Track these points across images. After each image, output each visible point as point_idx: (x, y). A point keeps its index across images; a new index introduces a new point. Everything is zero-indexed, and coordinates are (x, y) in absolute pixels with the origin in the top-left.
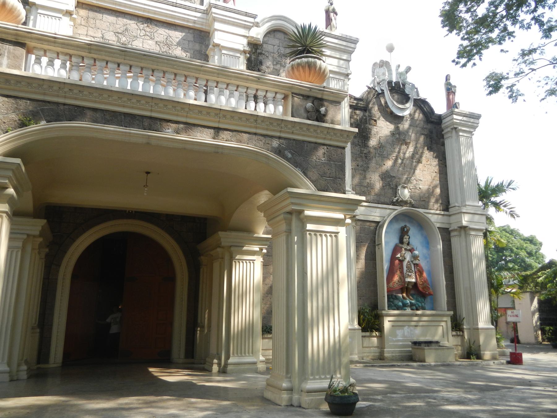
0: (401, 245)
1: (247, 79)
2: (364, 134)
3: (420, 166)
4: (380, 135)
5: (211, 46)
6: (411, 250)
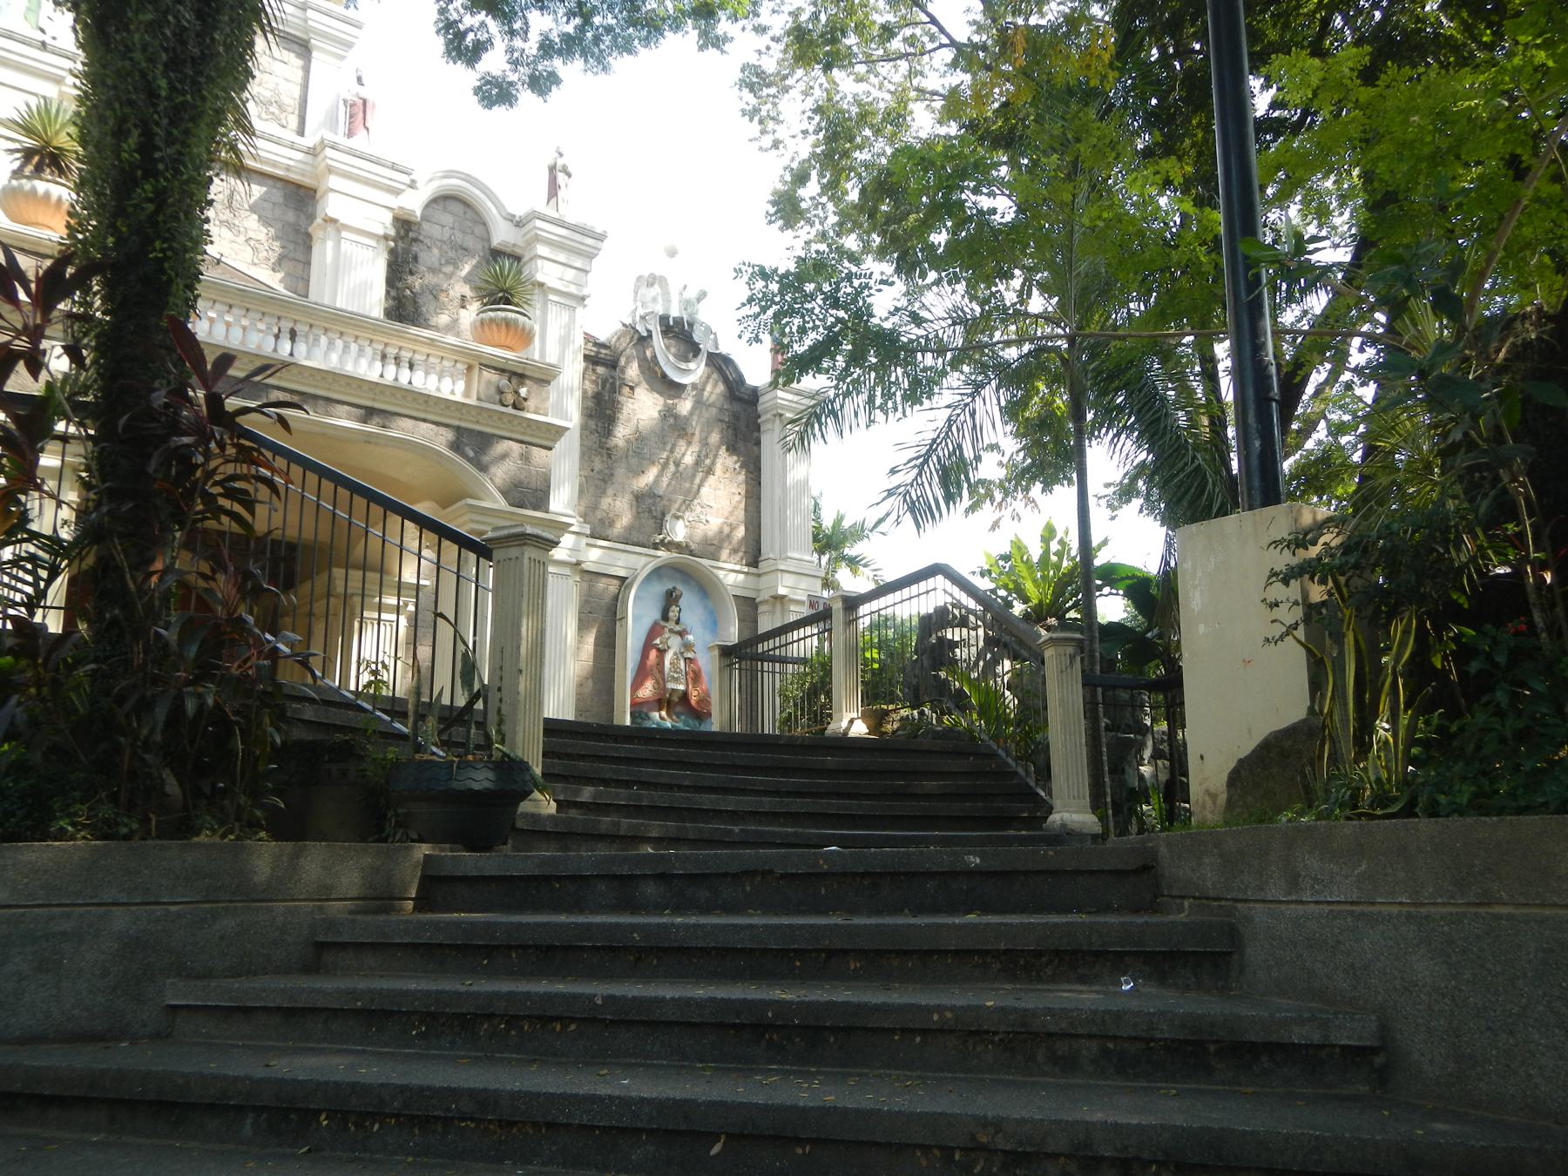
0: (663, 623)
1: (415, 341)
2: (608, 412)
3: (712, 479)
4: (640, 416)
5: (319, 220)
6: (681, 634)
